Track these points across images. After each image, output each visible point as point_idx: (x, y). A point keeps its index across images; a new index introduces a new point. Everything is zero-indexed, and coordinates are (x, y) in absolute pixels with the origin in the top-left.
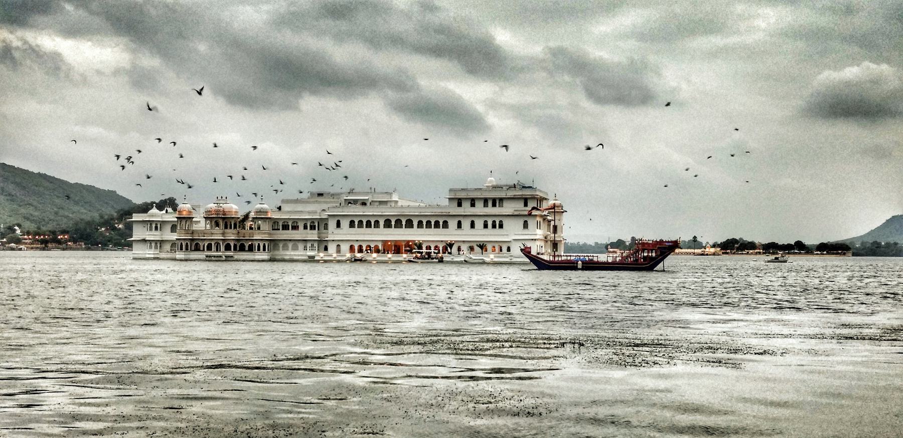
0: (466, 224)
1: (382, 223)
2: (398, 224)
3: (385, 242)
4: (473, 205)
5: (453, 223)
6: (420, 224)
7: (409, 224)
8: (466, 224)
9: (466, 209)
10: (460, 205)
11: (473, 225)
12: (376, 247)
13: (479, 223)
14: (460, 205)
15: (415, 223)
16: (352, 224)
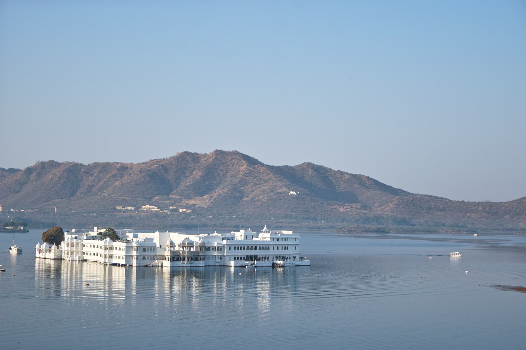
0: (276, 248)
1: (246, 248)
2: (252, 248)
3: (247, 256)
4: (278, 240)
5: (271, 248)
6: (260, 249)
7: (256, 248)
8: (276, 248)
9: (276, 243)
10: (274, 240)
11: (278, 249)
12: (244, 258)
13: (280, 248)
14: (274, 240)
15: (258, 248)
16: (235, 248)
